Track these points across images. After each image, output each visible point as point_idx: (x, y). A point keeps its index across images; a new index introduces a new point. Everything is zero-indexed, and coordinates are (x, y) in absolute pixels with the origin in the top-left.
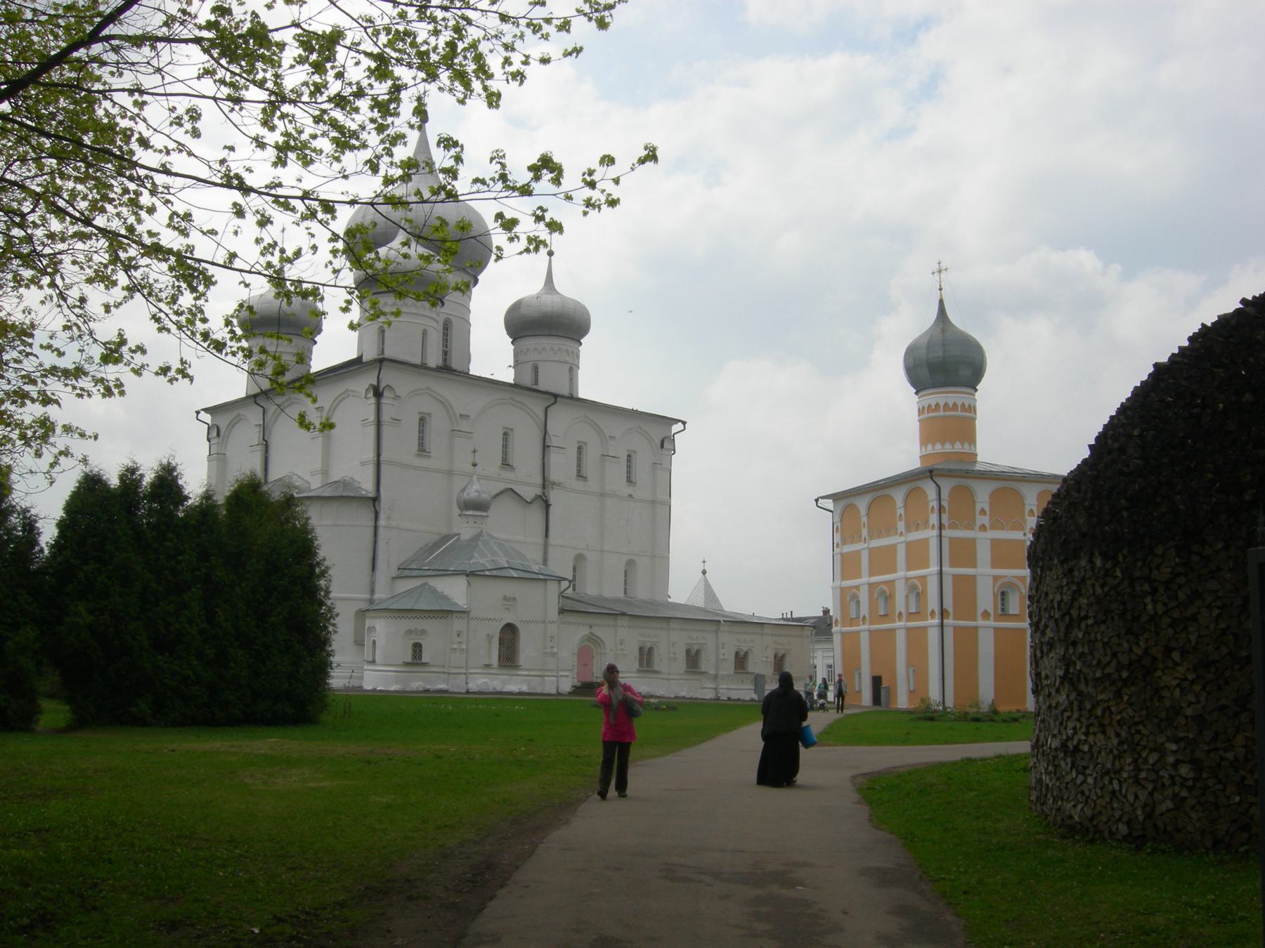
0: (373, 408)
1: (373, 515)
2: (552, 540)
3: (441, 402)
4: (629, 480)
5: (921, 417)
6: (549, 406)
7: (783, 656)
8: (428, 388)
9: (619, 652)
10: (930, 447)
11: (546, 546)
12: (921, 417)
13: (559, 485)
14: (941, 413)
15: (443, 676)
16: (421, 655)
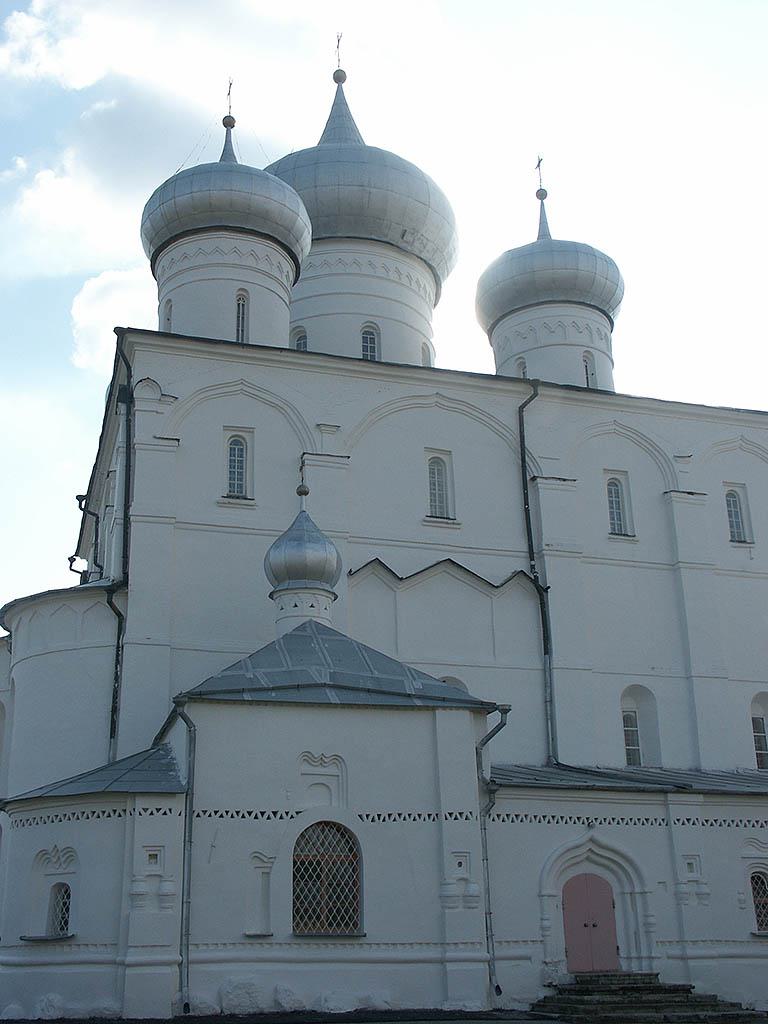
4: (738, 539)
11: (547, 671)
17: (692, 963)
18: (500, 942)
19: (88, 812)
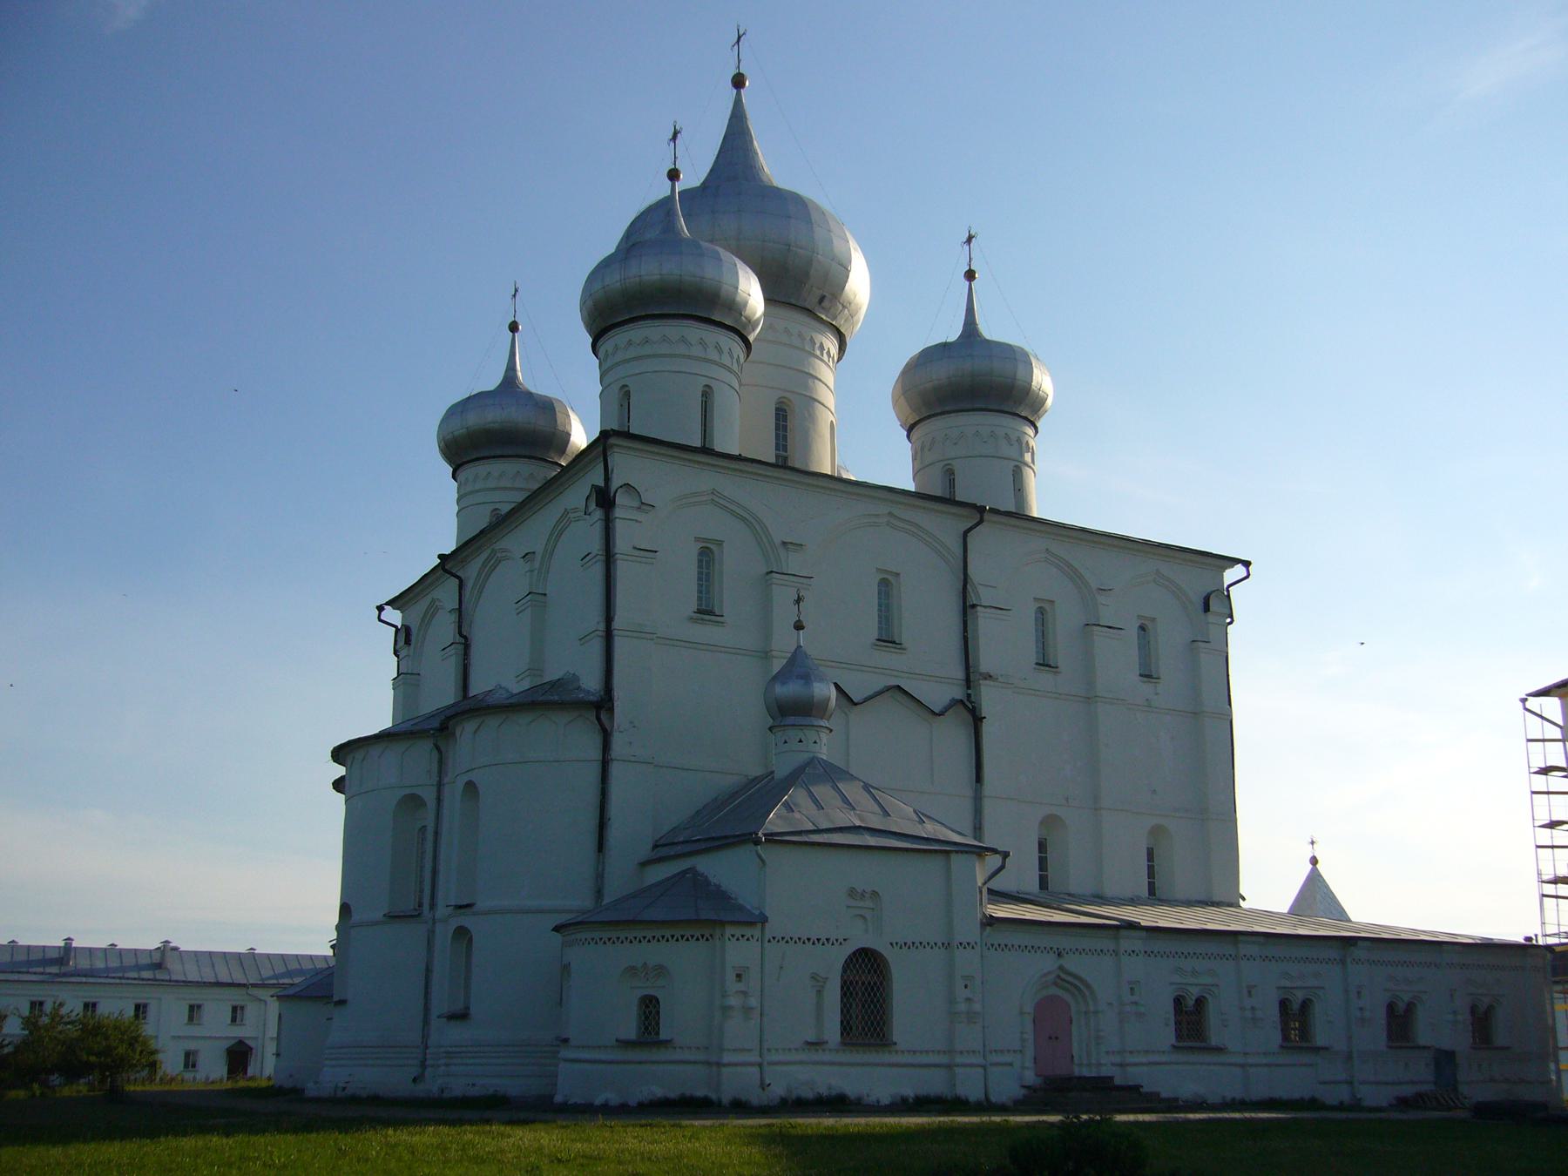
0: (598, 529)
1: (597, 739)
3: (744, 519)
7: (1490, 1010)
11: (978, 799)
17: (1130, 1069)
18: (769, 1050)
19: (678, 935)
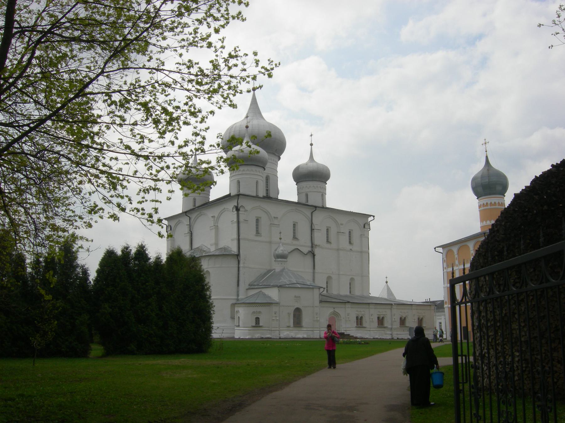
0: (235, 216)
1: (237, 263)
2: (316, 271)
3: (266, 212)
4: (350, 243)
5: (481, 209)
6: (313, 212)
7: (422, 319)
8: (259, 206)
9: (347, 319)
10: (484, 222)
11: (314, 273)
12: (481, 209)
13: (319, 246)
14: (489, 207)
15: (268, 331)
16: (259, 323)
17: (347, 331)
